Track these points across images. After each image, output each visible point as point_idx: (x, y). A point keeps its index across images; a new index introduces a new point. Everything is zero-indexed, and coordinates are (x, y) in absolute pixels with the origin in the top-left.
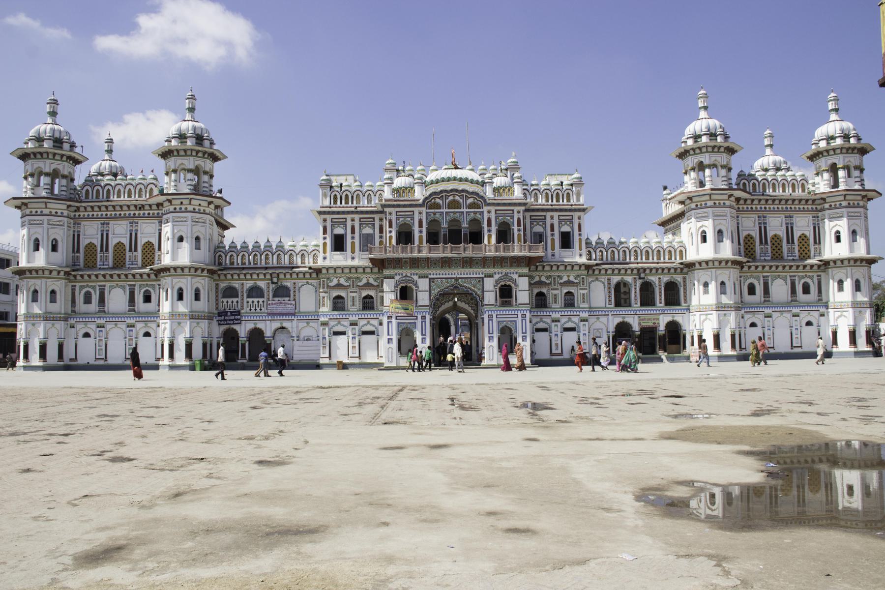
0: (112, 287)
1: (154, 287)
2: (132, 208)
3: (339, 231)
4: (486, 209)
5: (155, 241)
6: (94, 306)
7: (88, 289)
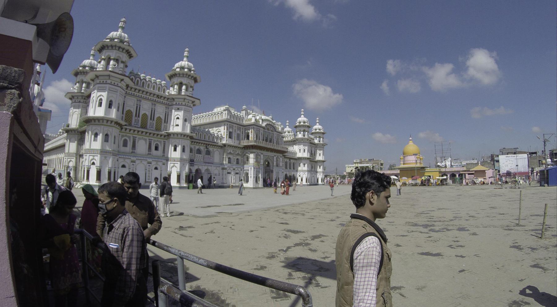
0: (140, 139)
1: (161, 142)
2: (155, 96)
3: (231, 130)
4: (275, 133)
5: (163, 117)
6: (129, 149)
7: (126, 138)
